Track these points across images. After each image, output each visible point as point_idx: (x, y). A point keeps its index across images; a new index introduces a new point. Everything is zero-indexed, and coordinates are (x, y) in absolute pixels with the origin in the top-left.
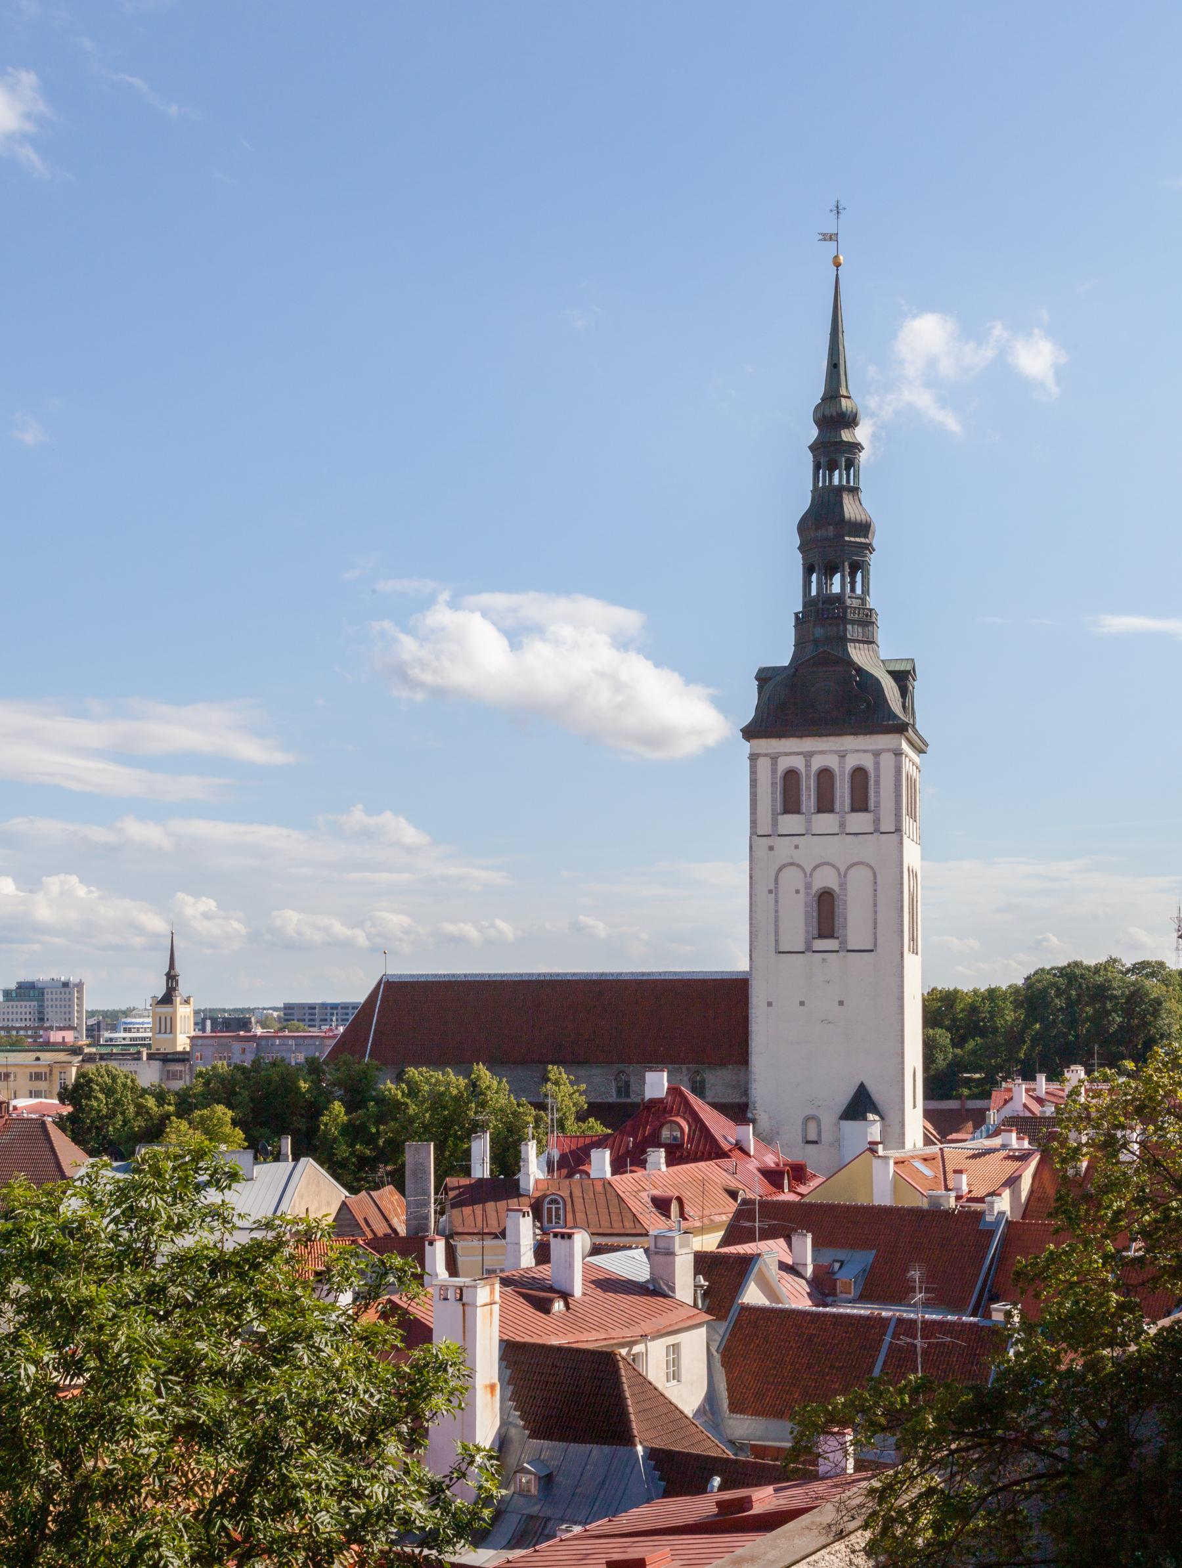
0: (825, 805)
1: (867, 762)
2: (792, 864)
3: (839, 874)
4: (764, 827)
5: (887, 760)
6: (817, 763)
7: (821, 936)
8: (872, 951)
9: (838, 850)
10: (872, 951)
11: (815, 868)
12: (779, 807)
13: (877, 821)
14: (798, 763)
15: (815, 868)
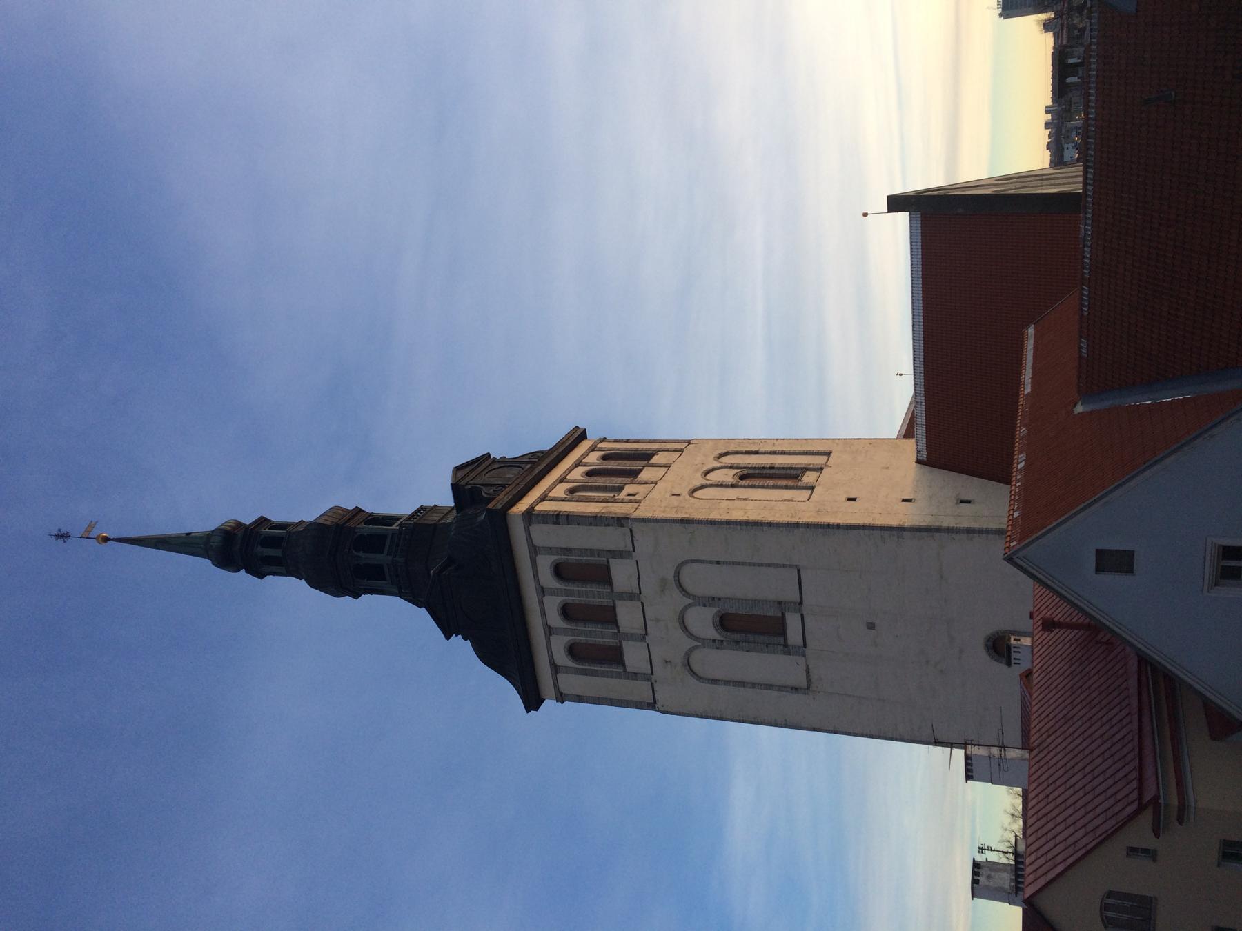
0: (607, 616)
1: (545, 564)
2: (688, 664)
3: (690, 606)
4: (641, 690)
5: (543, 535)
6: (555, 620)
7: (783, 633)
8: (799, 571)
9: (664, 607)
10: (799, 571)
11: (690, 635)
12: (614, 669)
13: (621, 555)
14: (559, 645)
15: (690, 635)
